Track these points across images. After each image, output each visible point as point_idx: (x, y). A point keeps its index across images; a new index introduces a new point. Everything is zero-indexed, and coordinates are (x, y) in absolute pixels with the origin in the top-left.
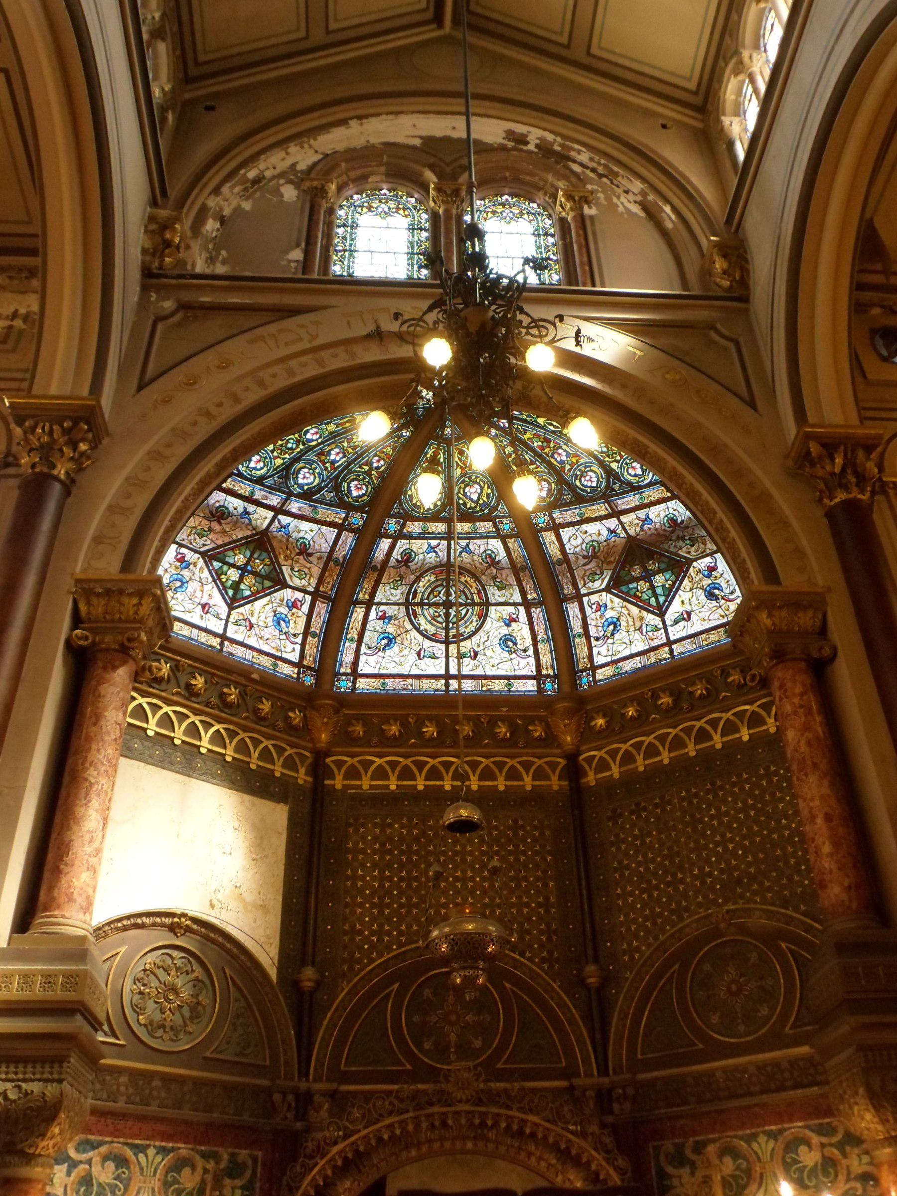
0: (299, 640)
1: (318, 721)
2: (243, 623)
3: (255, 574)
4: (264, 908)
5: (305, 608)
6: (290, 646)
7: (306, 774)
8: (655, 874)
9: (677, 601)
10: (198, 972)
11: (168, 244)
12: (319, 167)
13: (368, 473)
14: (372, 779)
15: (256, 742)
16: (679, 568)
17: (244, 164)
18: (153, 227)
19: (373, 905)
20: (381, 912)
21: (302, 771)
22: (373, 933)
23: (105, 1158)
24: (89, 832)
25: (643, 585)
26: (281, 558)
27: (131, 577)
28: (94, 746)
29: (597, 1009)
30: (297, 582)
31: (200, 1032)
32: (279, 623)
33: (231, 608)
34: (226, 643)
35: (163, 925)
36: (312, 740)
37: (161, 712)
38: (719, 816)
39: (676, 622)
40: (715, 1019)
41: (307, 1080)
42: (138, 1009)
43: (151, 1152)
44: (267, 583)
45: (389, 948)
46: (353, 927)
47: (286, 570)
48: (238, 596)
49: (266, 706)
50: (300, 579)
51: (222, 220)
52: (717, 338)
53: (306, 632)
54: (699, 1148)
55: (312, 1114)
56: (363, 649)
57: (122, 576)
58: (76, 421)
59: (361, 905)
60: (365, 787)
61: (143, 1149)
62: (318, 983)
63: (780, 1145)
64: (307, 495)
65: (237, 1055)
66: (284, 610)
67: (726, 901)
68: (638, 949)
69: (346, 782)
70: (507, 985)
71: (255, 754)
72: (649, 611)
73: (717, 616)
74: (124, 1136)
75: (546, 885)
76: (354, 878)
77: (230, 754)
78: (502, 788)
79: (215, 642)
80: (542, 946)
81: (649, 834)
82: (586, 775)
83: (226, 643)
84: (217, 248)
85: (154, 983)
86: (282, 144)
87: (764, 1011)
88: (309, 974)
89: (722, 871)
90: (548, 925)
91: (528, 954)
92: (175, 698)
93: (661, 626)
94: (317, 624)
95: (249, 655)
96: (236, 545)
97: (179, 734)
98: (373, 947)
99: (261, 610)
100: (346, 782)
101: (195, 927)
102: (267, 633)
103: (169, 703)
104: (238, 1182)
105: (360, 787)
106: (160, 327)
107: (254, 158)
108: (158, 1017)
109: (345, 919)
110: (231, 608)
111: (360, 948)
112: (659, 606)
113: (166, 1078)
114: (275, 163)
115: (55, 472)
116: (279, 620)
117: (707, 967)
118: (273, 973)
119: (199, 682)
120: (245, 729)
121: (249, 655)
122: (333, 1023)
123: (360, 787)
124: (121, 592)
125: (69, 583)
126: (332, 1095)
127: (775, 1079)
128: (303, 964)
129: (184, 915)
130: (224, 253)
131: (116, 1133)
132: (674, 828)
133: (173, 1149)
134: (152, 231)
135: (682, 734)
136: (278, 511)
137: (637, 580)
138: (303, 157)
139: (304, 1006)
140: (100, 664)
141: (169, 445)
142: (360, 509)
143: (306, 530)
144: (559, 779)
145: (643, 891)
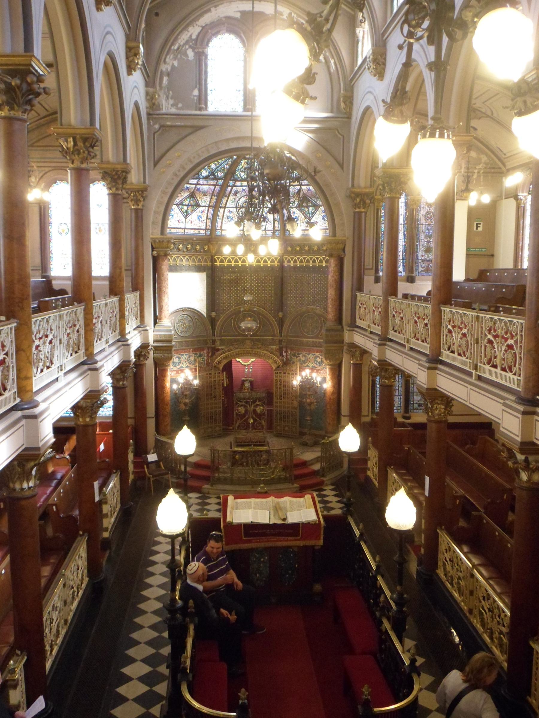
0: (205, 221)
1: (211, 247)
3: (191, 205)
4: (202, 300)
5: (206, 212)
6: (203, 224)
9: (314, 217)
10: (189, 319)
11: (154, 104)
12: (201, 36)
13: (224, 170)
15: (196, 258)
16: (316, 207)
17: (173, 44)
18: (148, 98)
21: (209, 262)
25: (306, 209)
26: (198, 199)
27: (165, 237)
29: (281, 323)
30: (203, 204)
33: (186, 218)
38: (314, 284)
44: (195, 207)
45: (232, 307)
47: (200, 202)
49: (198, 247)
50: (204, 201)
51: (168, 75)
52: (337, 133)
53: (207, 218)
54: (299, 354)
56: (224, 221)
57: (162, 236)
58: (142, 192)
61: (183, 355)
62: (216, 316)
64: (206, 178)
66: (200, 214)
76: (223, 290)
77: (191, 263)
79: (183, 231)
80: (269, 307)
84: (168, 91)
86: (185, 28)
88: (213, 314)
94: (210, 215)
96: (185, 198)
97: (178, 262)
98: (228, 307)
99: (193, 217)
103: (174, 254)
106: (156, 135)
107: (176, 39)
108: (182, 330)
110: (186, 218)
111: (225, 307)
112: (310, 217)
114: (184, 37)
115: (139, 207)
116: (199, 217)
118: (205, 315)
119: (181, 246)
120: (193, 255)
121: (192, 231)
124: (163, 241)
125: (149, 240)
127: (315, 345)
130: (171, 92)
131: (177, 353)
134: (149, 100)
136: (196, 185)
137: (305, 207)
138: (194, 31)
139: (213, 321)
141: (167, 188)
142: (221, 179)
143: (205, 188)
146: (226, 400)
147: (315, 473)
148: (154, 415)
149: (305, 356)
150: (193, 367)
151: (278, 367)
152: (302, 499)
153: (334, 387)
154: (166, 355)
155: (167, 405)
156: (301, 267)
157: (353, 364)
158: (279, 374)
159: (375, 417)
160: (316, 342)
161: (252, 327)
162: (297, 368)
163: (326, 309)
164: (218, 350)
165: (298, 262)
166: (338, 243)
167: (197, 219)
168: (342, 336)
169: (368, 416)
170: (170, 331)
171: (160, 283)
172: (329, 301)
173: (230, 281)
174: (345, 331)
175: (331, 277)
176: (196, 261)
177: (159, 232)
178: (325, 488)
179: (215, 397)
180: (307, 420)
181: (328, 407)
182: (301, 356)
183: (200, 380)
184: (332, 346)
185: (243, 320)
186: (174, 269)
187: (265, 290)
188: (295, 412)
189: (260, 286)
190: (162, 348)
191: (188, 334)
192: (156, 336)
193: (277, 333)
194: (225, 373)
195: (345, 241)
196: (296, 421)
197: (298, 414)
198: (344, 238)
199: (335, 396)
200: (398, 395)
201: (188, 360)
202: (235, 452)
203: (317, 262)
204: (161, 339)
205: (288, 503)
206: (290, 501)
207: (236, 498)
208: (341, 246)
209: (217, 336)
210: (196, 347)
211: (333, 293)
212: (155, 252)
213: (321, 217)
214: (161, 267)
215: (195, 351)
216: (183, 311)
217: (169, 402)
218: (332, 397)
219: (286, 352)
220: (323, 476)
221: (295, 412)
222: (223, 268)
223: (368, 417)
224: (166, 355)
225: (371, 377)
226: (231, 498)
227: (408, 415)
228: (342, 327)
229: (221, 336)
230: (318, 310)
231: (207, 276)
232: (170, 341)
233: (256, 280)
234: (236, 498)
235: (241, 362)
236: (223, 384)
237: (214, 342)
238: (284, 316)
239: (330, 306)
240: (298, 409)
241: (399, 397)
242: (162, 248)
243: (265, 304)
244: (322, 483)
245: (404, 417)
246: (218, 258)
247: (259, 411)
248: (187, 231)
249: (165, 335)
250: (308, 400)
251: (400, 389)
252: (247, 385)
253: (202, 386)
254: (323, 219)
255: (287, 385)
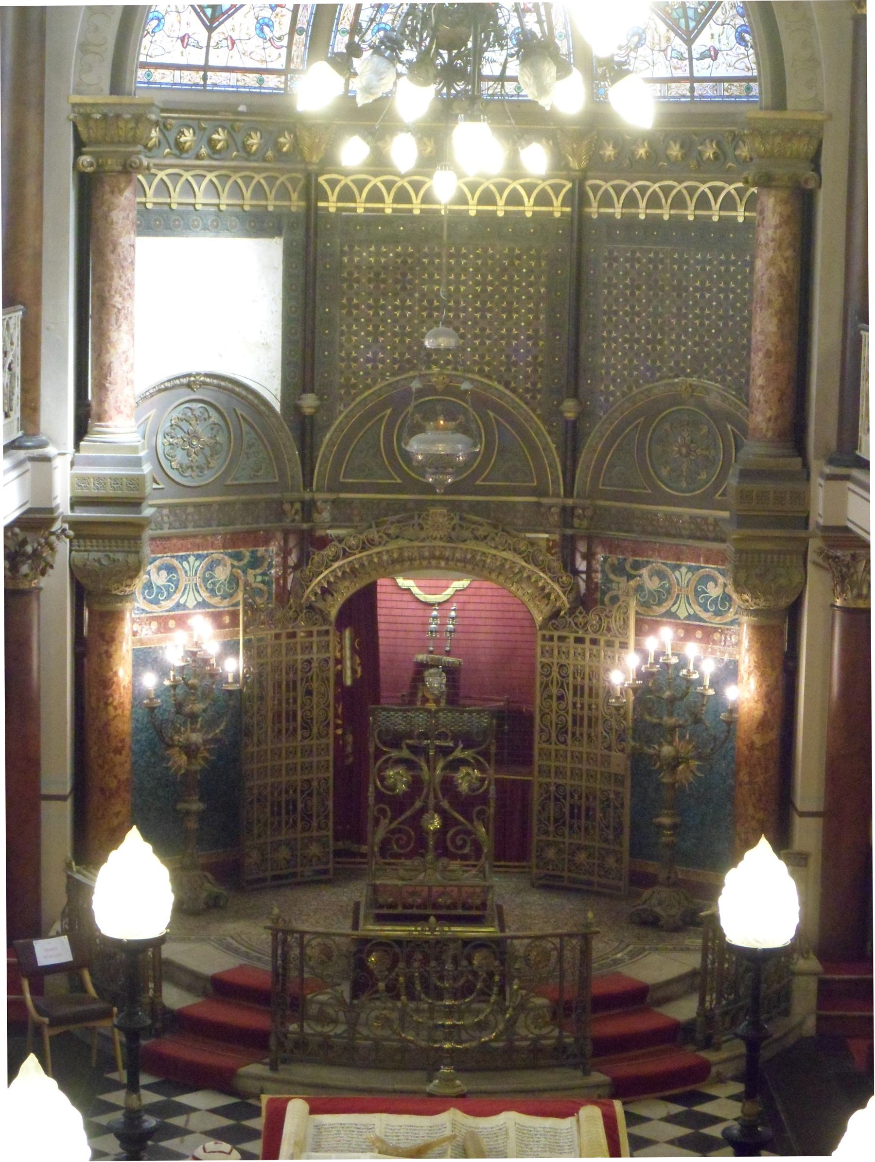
0: (285, 42)
2: (224, 43)
4: (266, 346)
6: (276, 52)
7: (300, 198)
8: (639, 328)
9: (706, 32)
10: (215, 417)
14: (367, 200)
15: (248, 180)
19: (368, 334)
20: (376, 340)
21: (294, 196)
22: (368, 360)
23: (159, 569)
24: (124, 353)
27: (125, 100)
28: (116, 274)
29: (572, 439)
31: (218, 466)
32: (262, 30)
33: (210, 29)
34: (209, 74)
35: (182, 385)
36: (303, 160)
37: (156, 181)
38: (702, 289)
39: (703, 57)
40: (664, 472)
41: (311, 490)
42: (170, 458)
43: (192, 559)
46: (349, 354)
48: (217, 14)
49: (255, 141)
54: (637, 566)
55: (316, 516)
57: (114, 99)
59: (356, 333)
60: (360, 211)
61: (186, 558)
62: (317, 409)
63: (696, 578)
65: (251, 478)
67: (694, 372)
68: (612, 394)
69: (340, 205)
70: (491, 414)
71: (248, 194)
72: (677, 34)
73: (742, 66)
74: (171, 551)
75: (536, 318)
76: (350, 306)
78: (501, 214)
79: (196, 77)
80: (527, 377)
81: (639, 288)
82: (589, 205)
83: (209, 74)
85: (180, 434)
87: (704, 476)
88: (309, 402)
89: (696, 344)
90: (535, 358)
91: (513, 385)
92: (167, 161)
93: (686, 55)
95: (233, 78)
97: (176, 199)
98: (367, 374)
100: (340, 205)
101: (208, 380)
102: (249, 46)
103: (161, 167)
104: (259, 571)
105: (354, 210)
108: (186, 461)
109: (342, 346)
110: (210, 29)
111: (355, 374)
113: (196, 505)
117: (667, 426)
118: (277, 406)
119: (188, 137)
120: (236, 169)
121: (233, 78)
122: (331, 443)
123: (354, 210)
124: (118, 116)
126: (334, 501)
128: (304, 391)
129: (198, 374)
131: (164, 550)
132: (662, 289)
133: (207, 556)
135: (685, 192)
139: (305, 429)
140: (107, 188)
144: (563, 204)
145: (626, 341)
146: (350, 738)
147: (675, 1034)
148: (67, 788)
149: (662, 575)
150: (224, 605)
151: (555, 615)
152: (567, 1123)
153: (767, 698)
154: (120, 556)
155: (118, 751)
156: (654, 222)
157: (844, 609)
158: (555, 643)
160: (705, 519)
161: (451, 456)
162: (626, 622)
163: (743, 390)
164: (323, 543)
165: (642, 204)
166: (790, 134)
167: (252, 32)
168: (802, 498)
170: (137, 462)
171: (103, 279)
172: (757, 360)
173: (377, 275)
174: (817, 481)
175: (767, 264)
176: (248, 194)
177: (106, 84)
178: (713, 1091)
179: (307, 725)
180: (660, 826)
181: (744, 777)
182: (645, 572)
183: (248, 659)
184: (765, 538)
185: (417, 429)
186: (158, 222)
187: (509, 311)
188: (617, 794)
189: (491, 296)
190: (107, 531)
191: (209, 477)
192: (80, 481)
193: (555, 481)
194: (347, 633)
195: (821, 125)
196: (618, 830)
197: (627, 802)
198: (818, 117)
199: (773, 735)
201: (205, 580)
202: (365, 944)
203: (716, 207)
204: (102, 493)
205: (512, 1134)
206: (521, 1129)
207: (315, 1109)
208: (802, 147)
209: (318, 490)
210: (239, 527)
211: (772, 327)
212: (85, 159)
213: (731, 33)
214: (106, 216)
215: (234, 542)
216: (189, 386)
217: (128, 740)
218: (758, 740)
219: (589, 557)
220: (709, 1044)
221: (617, 794)
222: (347, 223)
224: (120, 556)
226: (296, 1110)
228: (806, 465)
229: (336, 486)
230: (715, 392)
231: (288, 254)
232: (136, 504)
233: (477, 270)
234: (315, 1109)
235: (416, 590)
236: (339, 675)
237: (308, 509)
238: (584, 414)
239: (760, 381)
240: (628, 783)
242: (112, 143)
243: (509, 364)
244: (701, 1072)
246: (333, 183)
247: (464, 787)
248: (214, 78)
249: (116, 479)
250: (667, 750)
252: (435, 681)
253: (257, 678)
254: (741, 40)
255: (587, 688)
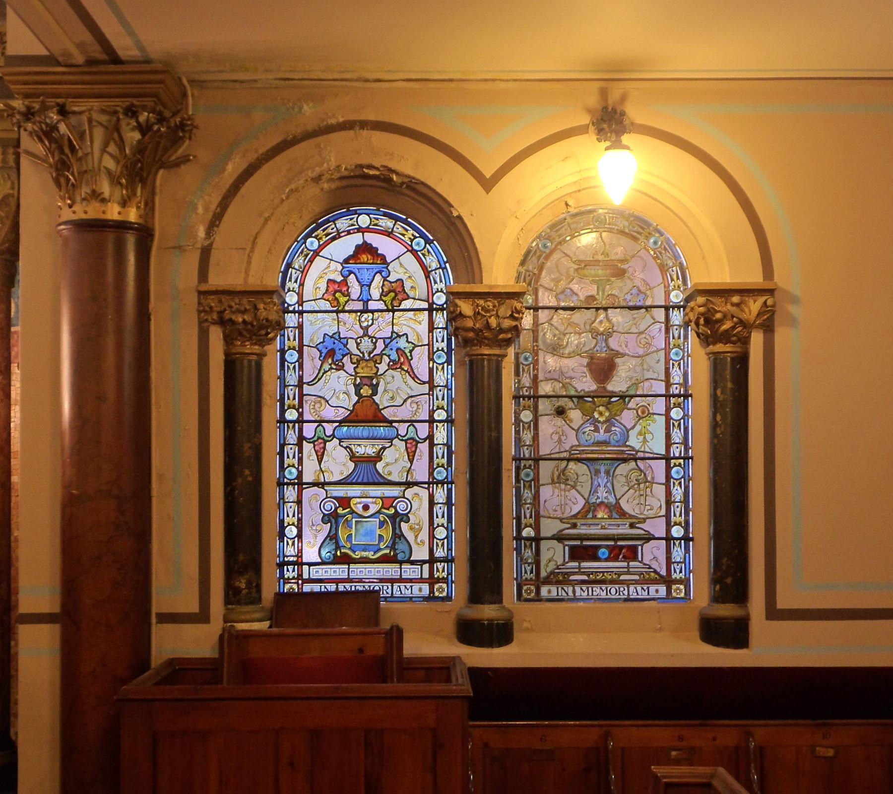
159: (255, 624)
169: (202, 617)
200: (432, 482)
223: (189, 630)
225: (216, 335)
227: (488, 612)
241: (440, 495)
245: (470, 632)
251: (441, 436)
